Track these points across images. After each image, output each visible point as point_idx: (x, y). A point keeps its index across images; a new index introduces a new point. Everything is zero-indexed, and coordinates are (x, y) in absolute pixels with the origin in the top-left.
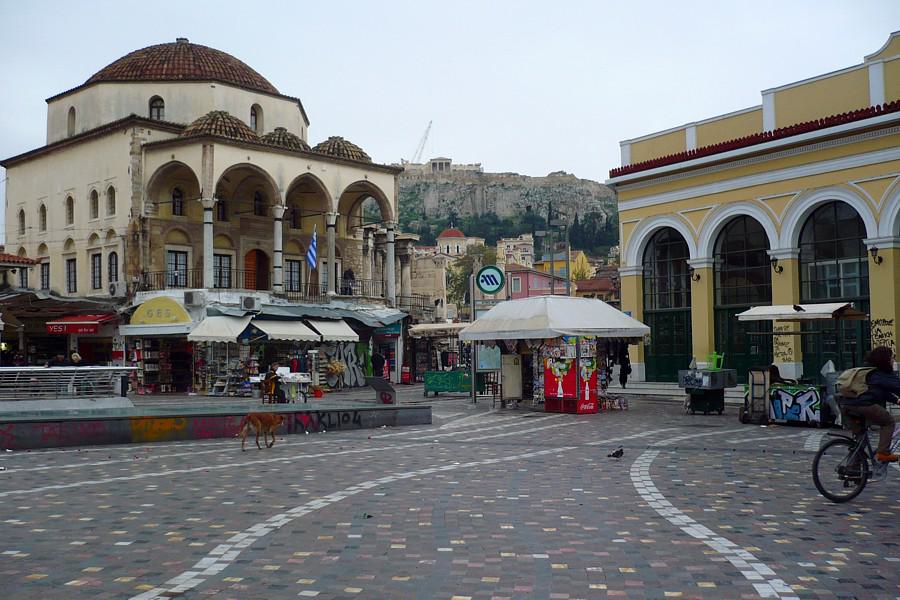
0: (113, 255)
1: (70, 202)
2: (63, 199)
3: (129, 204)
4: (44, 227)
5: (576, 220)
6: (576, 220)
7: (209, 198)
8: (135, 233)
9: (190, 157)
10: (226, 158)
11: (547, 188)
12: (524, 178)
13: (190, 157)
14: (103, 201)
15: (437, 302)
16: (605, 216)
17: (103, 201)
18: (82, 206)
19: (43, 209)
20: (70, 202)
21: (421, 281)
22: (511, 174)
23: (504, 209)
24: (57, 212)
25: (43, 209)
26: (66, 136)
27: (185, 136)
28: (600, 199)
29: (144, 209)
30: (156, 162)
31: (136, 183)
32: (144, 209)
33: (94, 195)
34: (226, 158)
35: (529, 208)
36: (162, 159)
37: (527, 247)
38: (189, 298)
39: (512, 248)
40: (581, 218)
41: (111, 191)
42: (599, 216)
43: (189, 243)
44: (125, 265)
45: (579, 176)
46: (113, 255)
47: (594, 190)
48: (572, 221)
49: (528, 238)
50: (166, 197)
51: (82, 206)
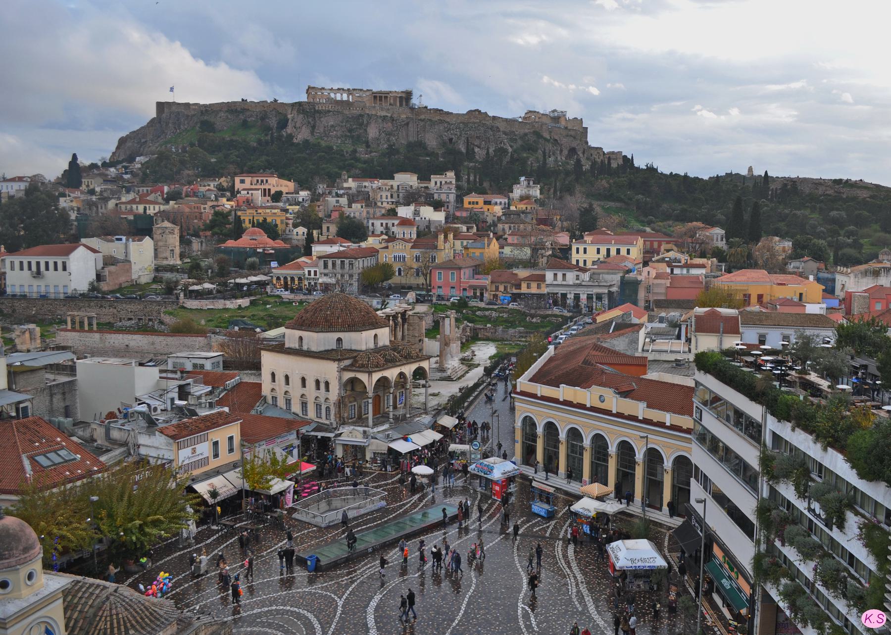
0: (328, 409)
1: (303, 380)
2: (301, 376)
3: (338, 391)
4: (287, 383)
5: (488, 153)
6: (488, 153)
7: (371, 394)
8: (339, 403)
9: (363, 377)
10: (376, 376)
11: (466, 124)
12: (448, 113)
13: (363, 377)
14: (322, 386)
15: (420, 341)
16: (510, 150)
17: (322, 386)
18: (311, 384)
19: (287, 377)
20: (303, 380)
21: (411, 328)
22: (437, 110)
23: (431, 141)
24: (295, 381)
25: (287, 377)
26: (297, 347)
27: (356, 360)
28: (505, 133)
29: (343, 393)
30: (348, 375)
31: (340, 384)
32: (343, 393)
33: (318, 382)
34: (376, 376)
35: (451, 140)
36: (350, 375)
37: (451, 186)
38: (365, 432)
39: (438, 184)
40: (491, 151)
41: (327, 384)
42: (505, 151)
43: (355, 401)
44: (335, 414)
45: (491, 114)
46: (328, 409)
47: (502, 127)
48: (484, 152)
49: (451, 175)
50: (349, 388)
51: (311, 384)
